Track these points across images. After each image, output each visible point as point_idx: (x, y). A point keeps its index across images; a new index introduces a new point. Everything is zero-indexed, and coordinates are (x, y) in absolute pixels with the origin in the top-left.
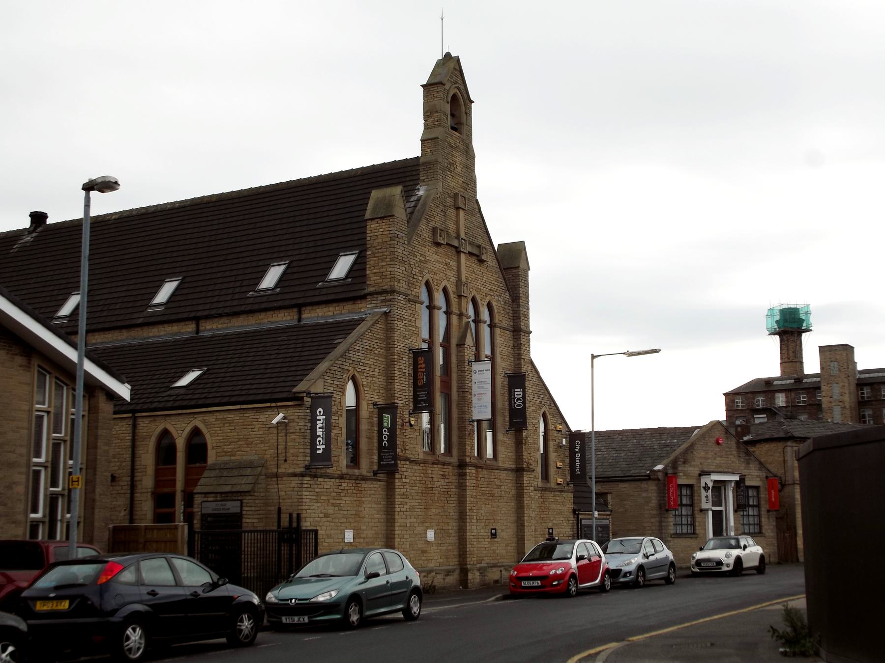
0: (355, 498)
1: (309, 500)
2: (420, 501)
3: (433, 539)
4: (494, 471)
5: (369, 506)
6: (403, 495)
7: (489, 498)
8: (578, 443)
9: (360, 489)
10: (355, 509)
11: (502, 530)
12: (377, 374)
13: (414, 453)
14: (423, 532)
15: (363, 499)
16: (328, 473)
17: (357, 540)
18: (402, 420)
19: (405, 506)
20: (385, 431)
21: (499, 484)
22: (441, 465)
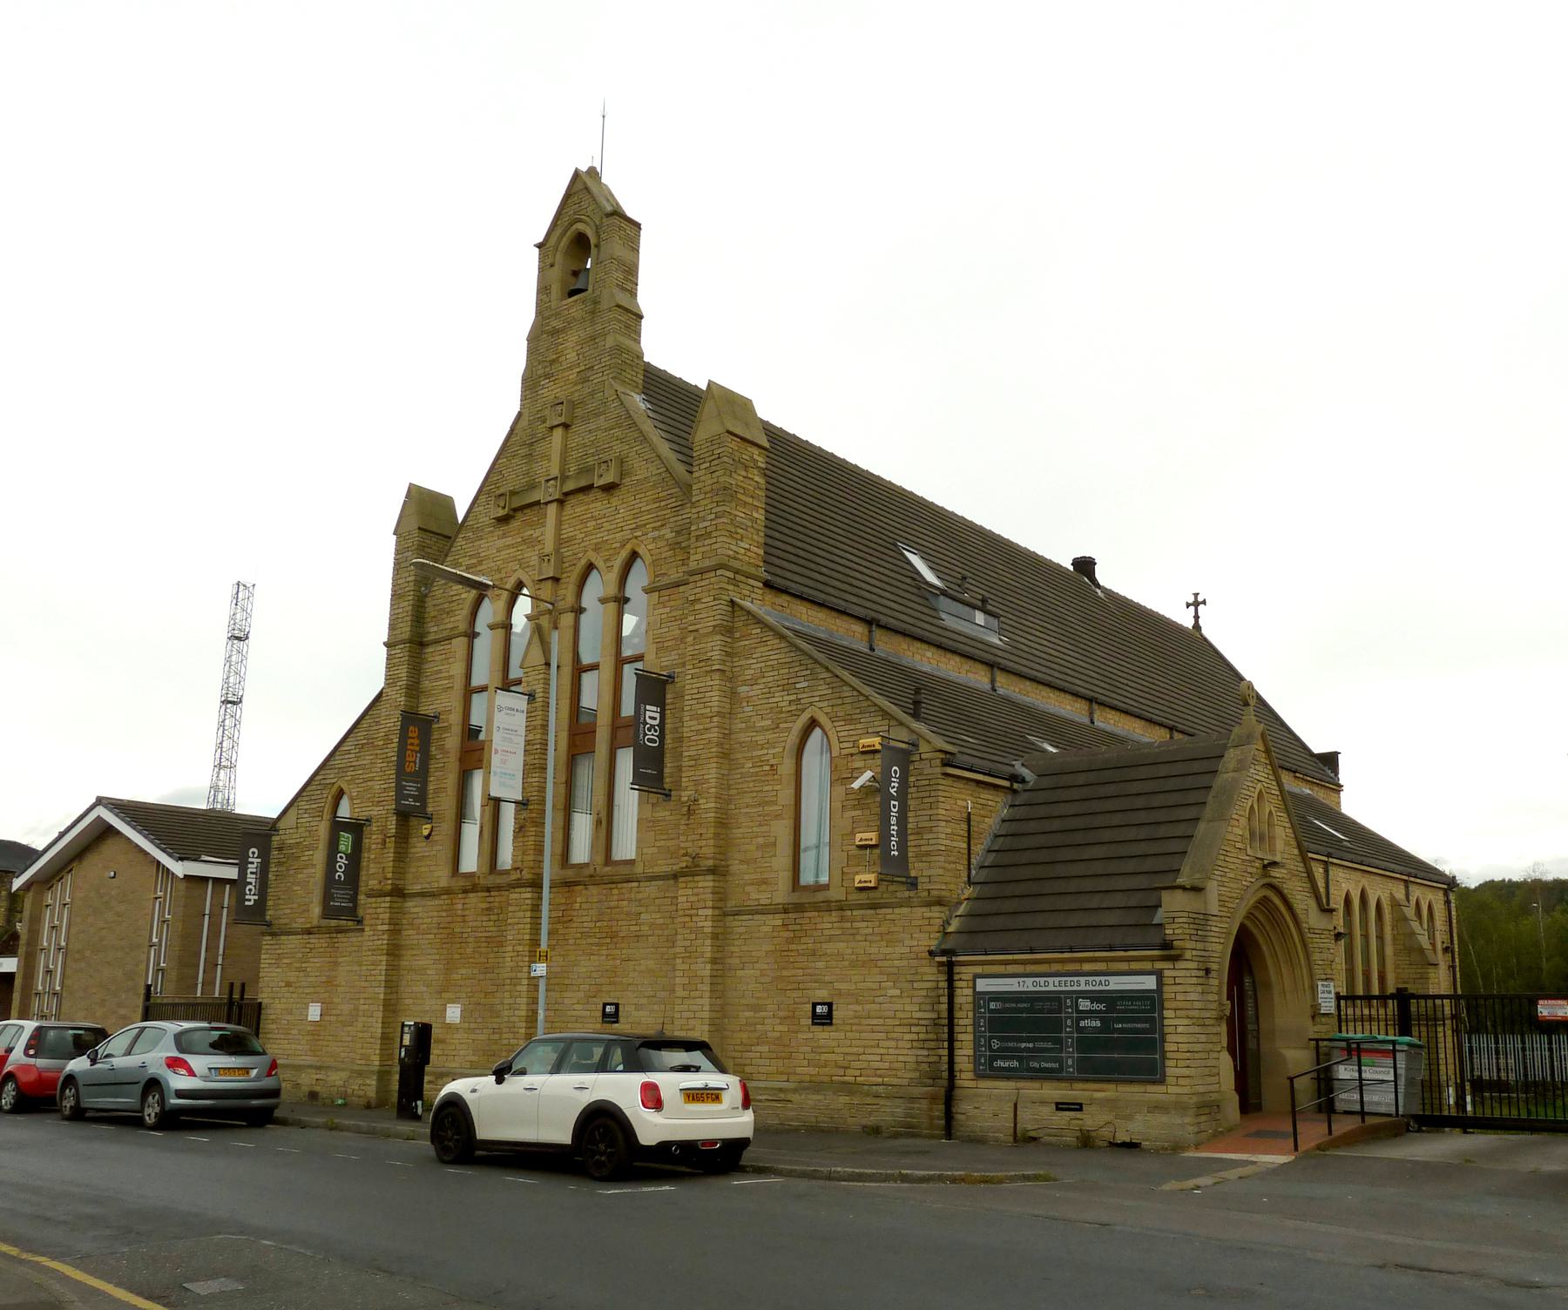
0: (328, 959)
1: (267, 965)
2: (437, 957)
3: (458, 1022)
4: (620, 886)
5: (349, 968)
8: (895, 772)
9: (336, 945)
11: (638, 1007)
14: (438, 1007)
15: (340, 960)
17: (327, 1018)
19: (379, 968)
20: (341, 858)
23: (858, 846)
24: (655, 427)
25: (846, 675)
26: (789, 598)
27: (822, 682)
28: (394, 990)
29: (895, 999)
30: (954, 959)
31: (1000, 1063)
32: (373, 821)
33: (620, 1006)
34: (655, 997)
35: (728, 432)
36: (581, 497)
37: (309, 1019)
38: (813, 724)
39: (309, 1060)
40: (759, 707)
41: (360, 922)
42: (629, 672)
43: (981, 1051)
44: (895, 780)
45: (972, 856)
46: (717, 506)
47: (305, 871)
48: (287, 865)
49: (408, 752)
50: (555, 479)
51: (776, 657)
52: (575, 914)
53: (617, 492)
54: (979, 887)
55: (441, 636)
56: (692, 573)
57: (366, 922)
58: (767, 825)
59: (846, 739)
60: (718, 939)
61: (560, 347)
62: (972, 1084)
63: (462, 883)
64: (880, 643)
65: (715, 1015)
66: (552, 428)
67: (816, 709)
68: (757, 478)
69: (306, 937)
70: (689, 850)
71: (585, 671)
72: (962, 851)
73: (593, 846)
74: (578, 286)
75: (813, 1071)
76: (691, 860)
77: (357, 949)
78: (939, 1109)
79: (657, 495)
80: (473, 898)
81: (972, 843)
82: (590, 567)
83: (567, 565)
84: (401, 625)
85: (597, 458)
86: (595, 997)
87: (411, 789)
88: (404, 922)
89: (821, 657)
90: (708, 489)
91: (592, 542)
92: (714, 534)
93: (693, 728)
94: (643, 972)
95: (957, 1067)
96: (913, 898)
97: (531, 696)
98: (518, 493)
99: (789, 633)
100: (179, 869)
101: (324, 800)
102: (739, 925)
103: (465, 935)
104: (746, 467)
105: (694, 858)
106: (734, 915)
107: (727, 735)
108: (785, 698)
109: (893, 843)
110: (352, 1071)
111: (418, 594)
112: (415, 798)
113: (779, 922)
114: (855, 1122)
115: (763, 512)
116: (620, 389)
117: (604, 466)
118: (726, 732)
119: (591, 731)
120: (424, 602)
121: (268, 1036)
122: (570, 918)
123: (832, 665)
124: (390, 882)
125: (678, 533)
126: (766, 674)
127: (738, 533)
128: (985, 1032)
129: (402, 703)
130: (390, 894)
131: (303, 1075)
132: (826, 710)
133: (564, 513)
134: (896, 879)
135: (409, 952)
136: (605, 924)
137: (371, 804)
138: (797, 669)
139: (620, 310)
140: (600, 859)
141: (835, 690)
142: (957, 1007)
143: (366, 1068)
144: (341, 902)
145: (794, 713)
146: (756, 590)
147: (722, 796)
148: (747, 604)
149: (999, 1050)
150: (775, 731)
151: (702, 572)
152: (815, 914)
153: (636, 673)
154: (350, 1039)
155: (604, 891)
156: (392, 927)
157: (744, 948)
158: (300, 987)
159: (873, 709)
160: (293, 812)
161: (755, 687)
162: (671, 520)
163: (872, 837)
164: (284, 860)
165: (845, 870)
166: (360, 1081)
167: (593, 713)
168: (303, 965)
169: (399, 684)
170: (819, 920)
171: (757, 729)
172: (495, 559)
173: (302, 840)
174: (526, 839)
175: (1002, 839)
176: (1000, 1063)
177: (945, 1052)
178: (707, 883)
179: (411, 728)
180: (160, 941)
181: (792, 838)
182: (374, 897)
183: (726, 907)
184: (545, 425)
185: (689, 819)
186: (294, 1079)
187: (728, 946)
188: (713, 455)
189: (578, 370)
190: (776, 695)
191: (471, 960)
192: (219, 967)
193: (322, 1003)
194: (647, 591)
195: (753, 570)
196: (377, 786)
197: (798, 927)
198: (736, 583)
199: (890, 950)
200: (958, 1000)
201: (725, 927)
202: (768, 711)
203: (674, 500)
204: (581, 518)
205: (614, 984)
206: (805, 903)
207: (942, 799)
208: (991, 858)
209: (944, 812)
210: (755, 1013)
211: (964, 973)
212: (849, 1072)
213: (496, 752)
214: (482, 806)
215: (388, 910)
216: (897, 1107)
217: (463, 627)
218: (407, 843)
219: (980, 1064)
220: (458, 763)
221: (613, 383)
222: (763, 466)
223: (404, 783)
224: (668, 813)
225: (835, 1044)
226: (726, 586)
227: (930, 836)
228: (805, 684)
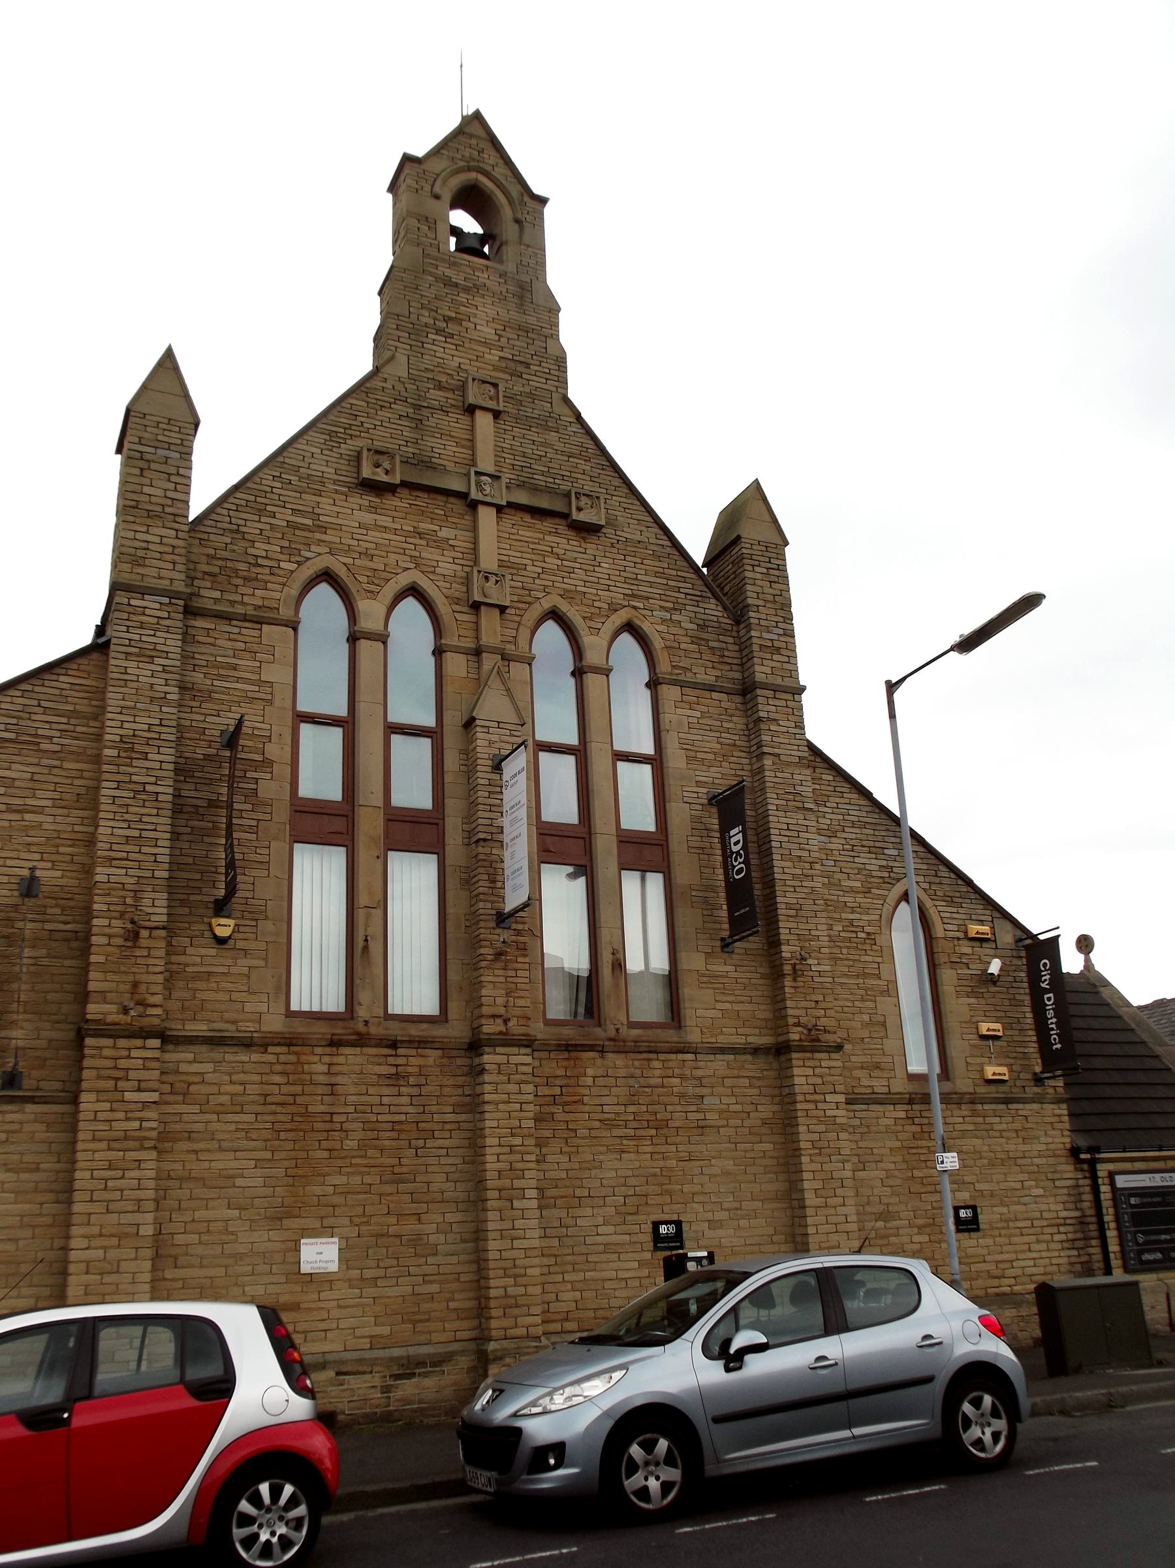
3: (334, 1267)
4: (662, 1057)
6: (126, 1138)
12: (49, 803)
18: (133, 922)
21: (690, 1090)
22: (377, 1046)
29: (1038, 1199)
30: (1097, 1156)
31: (1147, 1257)
33: (684, 1225)
36: (527, 518)
70: (803, 1020)
76: (805, 1031)
80: (351, 1057)
94: (715, 1176)
105: (810, 1030)
108: (873, 861)
113: (902, 1115)
136: (644, 1108)
149: (1146, 1243)
150: (867, 895)
155: (637, 1063)
161: (834, 840)
165: (969, 1060)
176: (1147, 1257)
177: (1097, 1250)
182: (110, 1037)
189: (501, 354)
199: (1027, 1147)
202: (856, 871)
205: (670, 1193)
211: (1103, 1169)
225: (984, 1251)
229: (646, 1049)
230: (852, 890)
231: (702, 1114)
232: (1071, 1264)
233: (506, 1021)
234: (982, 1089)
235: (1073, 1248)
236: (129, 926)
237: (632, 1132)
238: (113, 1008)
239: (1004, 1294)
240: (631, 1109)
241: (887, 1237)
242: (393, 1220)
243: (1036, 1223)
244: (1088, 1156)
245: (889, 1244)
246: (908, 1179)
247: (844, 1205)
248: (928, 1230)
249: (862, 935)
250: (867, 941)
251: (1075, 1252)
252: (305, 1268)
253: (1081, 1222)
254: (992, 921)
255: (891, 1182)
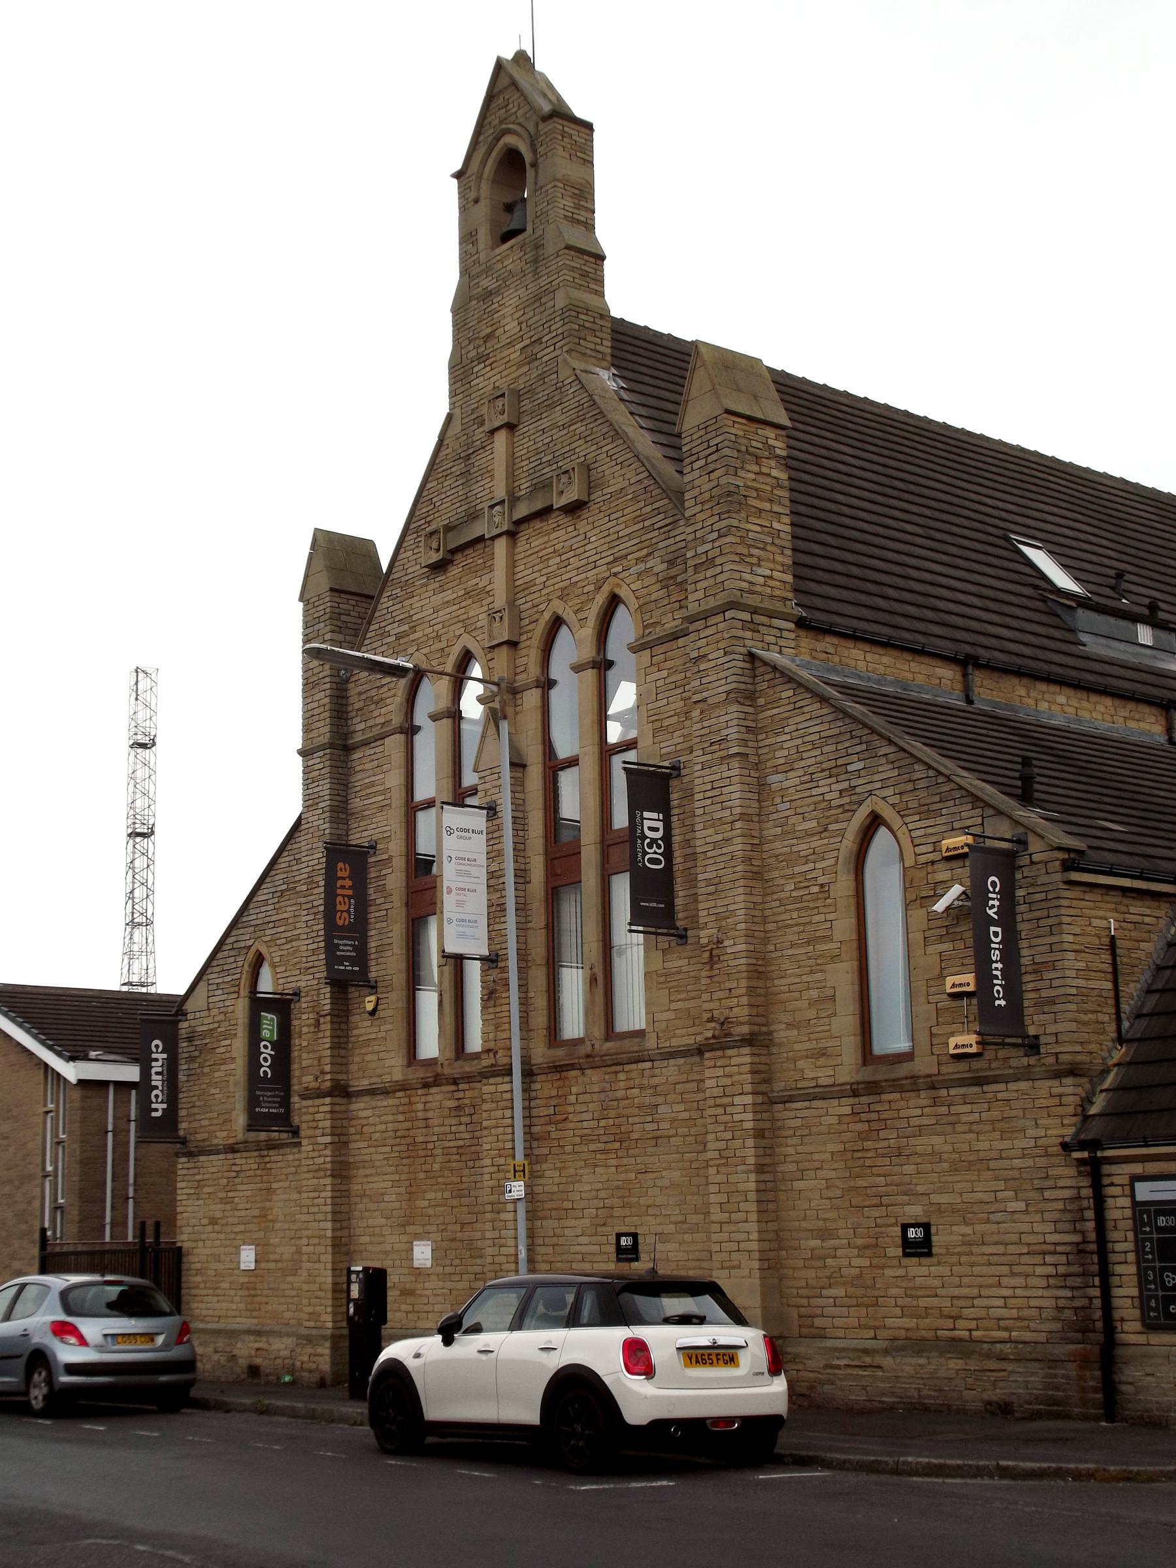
0: (259, 1185)
1: (185, 1197)
2: (396, 1177)
3: (429, 1264)
4: (627, 1067)
5: (285, 1197)
6: (319, 1170)
7: (609, 1146)
8: (994, 884)
9: (268, 1166)
10: (259, 1205)
11: (662, 1237)
13: (378, 1071)
14: (403, 1246)
15: (275, 1186)
16: (215, 1145)
17: (263, 1265)
19: (322, 1195)
21: (647, 1101)
22: (448, 1084)
23: (951, 995)
24: (631, 413)
25: (918, 748)
26: (835, 640)
27: (883, 760)
28: (344, 1224)
29: (1016, 1216)
30: (1099, 1154)
32: (303, 994)
33: (639, 1237)
34: (684, 1222)
35: (728, 412)
36: (537, 524)
37: (243, 1267)
38: (875, 822)
39: (246, 1323)
40: (798, 803)
41: (296, 1132)
42: (617, 762)
43: (1150, 1290)
44: (994, 896)
45: (1122, 1000)
46: (720, 520)
47: (223, 1068)
48: (199, 1060)
49: (339, 899)
50: (502, 502)
51: (816, 729)
52: (571, 1109)
53: (585, 513)
54: (1135, 1045)
55: (371, 735)
56: (692, 619)
57: (303, 1133)
58: (822, 971)
59: (923, 840)
60: (763, 1137)
61: (495, 316)
62: (1142, 1339)
63: (421, 1073)
64: (981, 690)
65: (766, 1245)
66: (492, 432)
67: (881, 802)
68: (775, 473)
69: (230, 1156)
71: (562, 769)
72: (1105, 994)
73: (588, 1012)
74: (515, 225)
75: (911, 1323)
76: (718, 1027)
77: (293, 1170)
78: (1093, 1377)
79: (638, 513)
80: (437, 1095)
81: (1120, 980)
82: (557, 622)
83: (526, 622)
84: (318, 724)
85: (555, 466)
86: (604, 1225)
87: (345, 948)
88: (352, 1130)
89: (877, 722)
90: (707, 496)
91: (557, 586)
92: (718, 561)
93: (708, 840)
95: (1117, 1315)
96: (1034, 1066)
97: (492, 810)
98: (455, 527)
99: (832, 692)
100: (71, 1071)
101: (239, 970)
102: (792, 1116)
103: (430, 1146)
104: (757, 457)
106: (785, 1102)
107: (757, 845)
108: (834, 787)
109: (997, 988)
110: (299, 1337)
111: (338, 680)
112: (353, 961)
113: (847, 1110)
114: (974, 1397)
115: (787, 520)
116: (578, 365)
117: (564, 479)
118: (756, 841)
119: (575, 853)
120: (346, 690)
121: (194, 1292)
122: (565, 1116)
123: (895, 733)
124: (328, 1077)
125: (671, 563)
126: (805, 755)
127: (752, 556)
128: (1153, 1261)
129: (327, 832)
130: (330, 1094)
131: (239, 1345)
132: (891, 800)
133: (518, 550)
134: (1008, 1040)
135: (361, 1172)
136: (611, 1122)
137: (298, 972)
138: (847, 744)
139: (572, 253)
140: (598, 1031)
141: (903, 771)
142: (1110, 1225)
143: (314, 1332)
144: (269, 1108)
145: (847, 808)
146: (785, 634)
147: (756, 934)
148: (773, 656)
151: (705, 616)
152: (896, 1096)
153: (625, 769)
154: (294, 1293)
155: (607, 1077)
156: (336, 1139)
157: (800, 1149)
158: (227, 1224)
159: (957, 794)
160: (202, 986)
161: (791, 774)
162: (661, 545)
163: (967, 980)
164: (197, 1053)
165: (934, 1031)
166: (309, 1350)
167: (575, 826)
168: (230, 1194)
169: (321, 805)
170: (902, 1103)
171: (798, 834)
172: (432, 623)
173: (216, 1025)
174: (498, 1009)
175: (1168, 973)
177: (1096, 1292)
178: (742, 1058)
179: (340, 865)
180: (56, 1169)
181: (857, 987)
182: (310, 1098)
183: (772, 1091)
184: (481, 430)
185: (711, 969)
186: (228, 1349)
187: (780, 1145)
188: (709, 447)
189: (521, 345)
190: (821, 783)
191: (440, 1180)
192: (131, 1201)
193: (257, 1245)
194: (635, 649)
195: (778, 606)
196: (304, 946)
197: (874, 1116)
198: (752, 627)
199: (1006, 1144)
200: (1112, 1214)
201: (773, 1120)
203: (662, 516)
204: (540, 554)
206: (881, 1081)
207: (1068, 920)
208: (1152, 1001)
209: (1070, 938)
210: (822, 1240)
211: (1119, 1174)
212: (961, 1323)
213: (449, 891)
214: (439, 966)
215: (328, 1116)
216: (1033, 1374)
217: (397, 720)
218: (347, 1022)
219: (1151, 1309)
220: (404, 909)
221: (569, 359)
222: (784, 453)
223: (336, 941)
224: (684, 962)
225: (937, 1283)
226: (740, 633)
227: (1053, 975)
228: (860, 765)
229: (611, 1062)
230: (808, 834)
231: (656, 1125)
232: (1059, 1309)
233: (496, 1053)
234: (949, 1069)
235: (1064, 1287)
236: (316, 1016)
237: (602, 1146)
238: (310, 1078)
239: (962, 1340)
240: (603, 1123)
241: (824, 1258)
242: (458, 1227)
243: (1012, 1249)
244: (1085, 1154)
245: (825, 1267)
246: (851, 1189)
247: (747, 1221)
248: (869, 1252)
249: (815, 889)
250: (820, 896)
251: (1068, 1293)
252: (416, 1264)
253: (1080, 1250)
254: (982, 824)
255: (830, 1194)
